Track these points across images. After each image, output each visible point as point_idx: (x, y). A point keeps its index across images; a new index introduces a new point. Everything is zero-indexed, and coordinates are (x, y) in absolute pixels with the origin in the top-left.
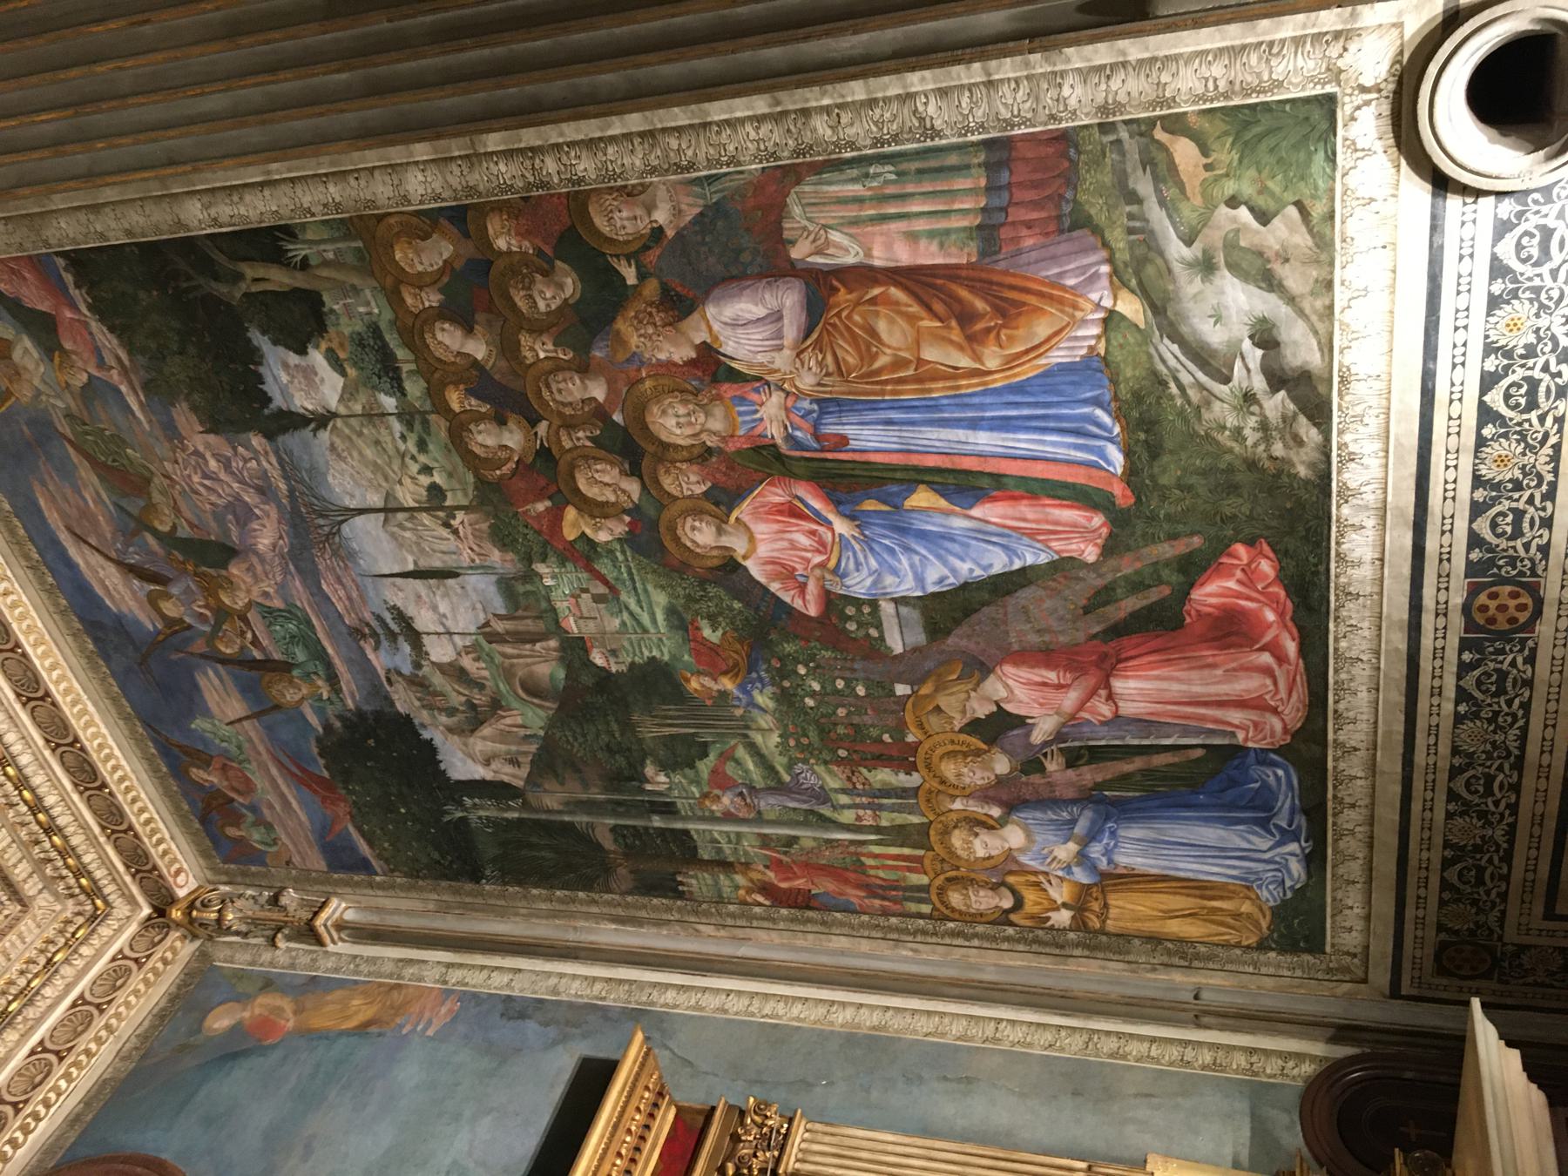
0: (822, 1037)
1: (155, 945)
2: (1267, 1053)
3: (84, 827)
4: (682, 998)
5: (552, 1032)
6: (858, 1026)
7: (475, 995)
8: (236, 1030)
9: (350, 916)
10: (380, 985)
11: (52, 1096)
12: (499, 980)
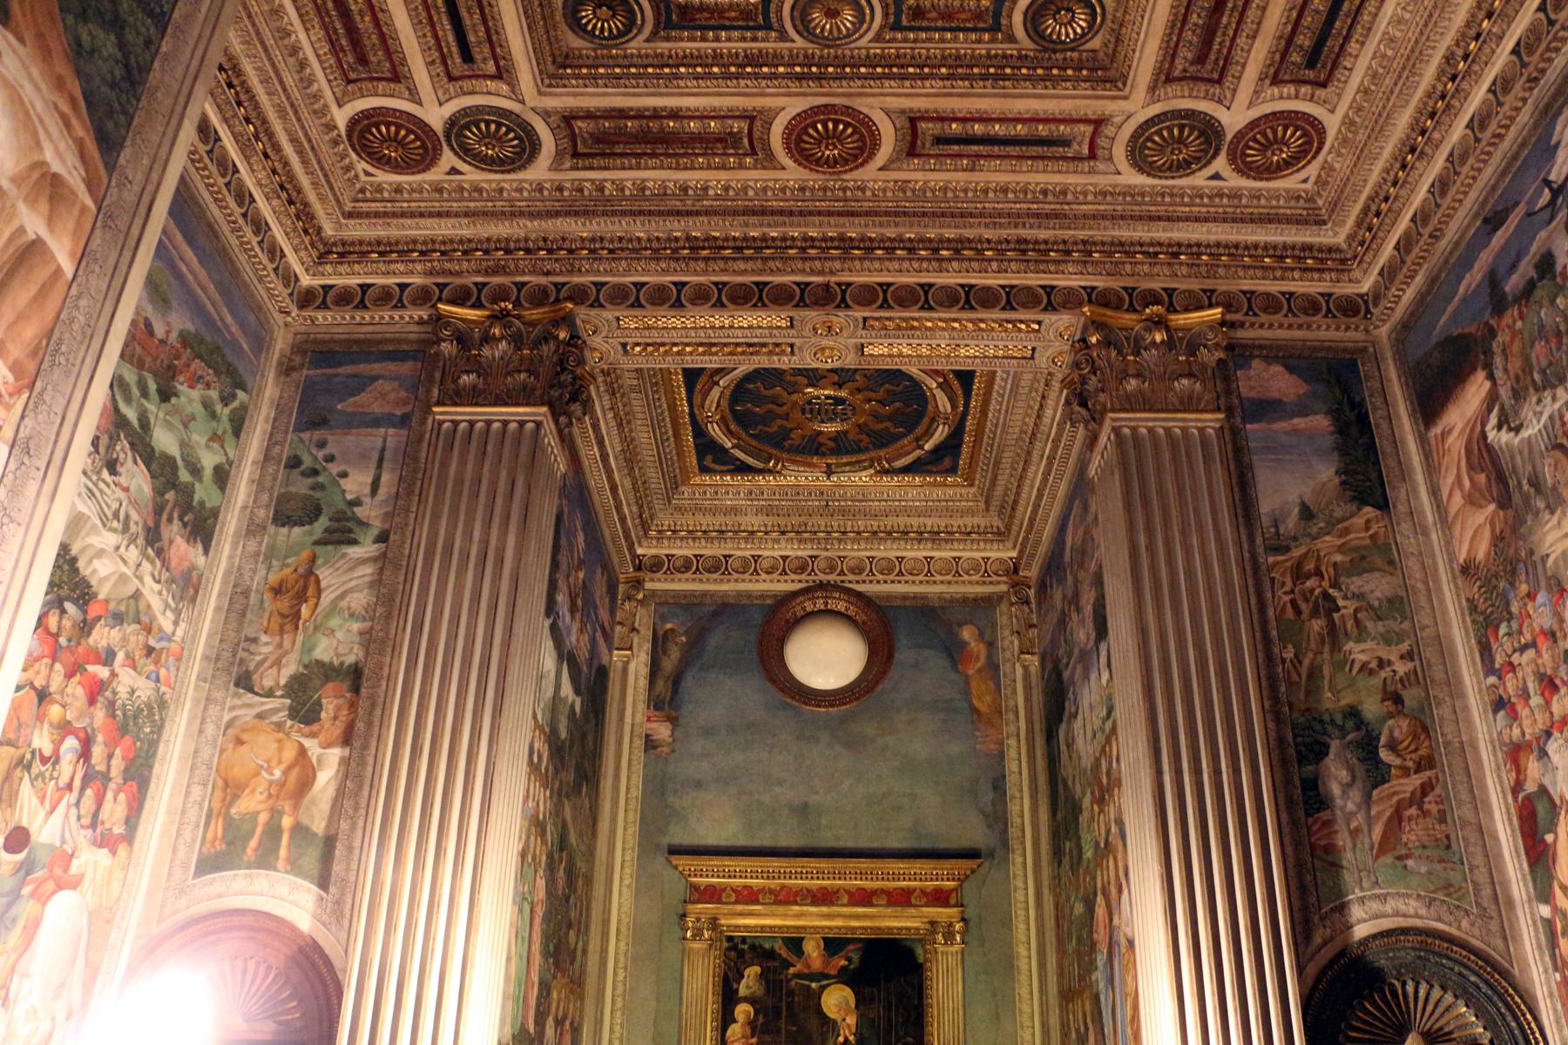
0: (1009, 944)
1: (996, 574)
3: (1022, 524)
4: (1019, 866)
5: (989, 808)
6: (1018, 959)
8: (965, 644)
9: (1033, 670)
12: (1014, 766)
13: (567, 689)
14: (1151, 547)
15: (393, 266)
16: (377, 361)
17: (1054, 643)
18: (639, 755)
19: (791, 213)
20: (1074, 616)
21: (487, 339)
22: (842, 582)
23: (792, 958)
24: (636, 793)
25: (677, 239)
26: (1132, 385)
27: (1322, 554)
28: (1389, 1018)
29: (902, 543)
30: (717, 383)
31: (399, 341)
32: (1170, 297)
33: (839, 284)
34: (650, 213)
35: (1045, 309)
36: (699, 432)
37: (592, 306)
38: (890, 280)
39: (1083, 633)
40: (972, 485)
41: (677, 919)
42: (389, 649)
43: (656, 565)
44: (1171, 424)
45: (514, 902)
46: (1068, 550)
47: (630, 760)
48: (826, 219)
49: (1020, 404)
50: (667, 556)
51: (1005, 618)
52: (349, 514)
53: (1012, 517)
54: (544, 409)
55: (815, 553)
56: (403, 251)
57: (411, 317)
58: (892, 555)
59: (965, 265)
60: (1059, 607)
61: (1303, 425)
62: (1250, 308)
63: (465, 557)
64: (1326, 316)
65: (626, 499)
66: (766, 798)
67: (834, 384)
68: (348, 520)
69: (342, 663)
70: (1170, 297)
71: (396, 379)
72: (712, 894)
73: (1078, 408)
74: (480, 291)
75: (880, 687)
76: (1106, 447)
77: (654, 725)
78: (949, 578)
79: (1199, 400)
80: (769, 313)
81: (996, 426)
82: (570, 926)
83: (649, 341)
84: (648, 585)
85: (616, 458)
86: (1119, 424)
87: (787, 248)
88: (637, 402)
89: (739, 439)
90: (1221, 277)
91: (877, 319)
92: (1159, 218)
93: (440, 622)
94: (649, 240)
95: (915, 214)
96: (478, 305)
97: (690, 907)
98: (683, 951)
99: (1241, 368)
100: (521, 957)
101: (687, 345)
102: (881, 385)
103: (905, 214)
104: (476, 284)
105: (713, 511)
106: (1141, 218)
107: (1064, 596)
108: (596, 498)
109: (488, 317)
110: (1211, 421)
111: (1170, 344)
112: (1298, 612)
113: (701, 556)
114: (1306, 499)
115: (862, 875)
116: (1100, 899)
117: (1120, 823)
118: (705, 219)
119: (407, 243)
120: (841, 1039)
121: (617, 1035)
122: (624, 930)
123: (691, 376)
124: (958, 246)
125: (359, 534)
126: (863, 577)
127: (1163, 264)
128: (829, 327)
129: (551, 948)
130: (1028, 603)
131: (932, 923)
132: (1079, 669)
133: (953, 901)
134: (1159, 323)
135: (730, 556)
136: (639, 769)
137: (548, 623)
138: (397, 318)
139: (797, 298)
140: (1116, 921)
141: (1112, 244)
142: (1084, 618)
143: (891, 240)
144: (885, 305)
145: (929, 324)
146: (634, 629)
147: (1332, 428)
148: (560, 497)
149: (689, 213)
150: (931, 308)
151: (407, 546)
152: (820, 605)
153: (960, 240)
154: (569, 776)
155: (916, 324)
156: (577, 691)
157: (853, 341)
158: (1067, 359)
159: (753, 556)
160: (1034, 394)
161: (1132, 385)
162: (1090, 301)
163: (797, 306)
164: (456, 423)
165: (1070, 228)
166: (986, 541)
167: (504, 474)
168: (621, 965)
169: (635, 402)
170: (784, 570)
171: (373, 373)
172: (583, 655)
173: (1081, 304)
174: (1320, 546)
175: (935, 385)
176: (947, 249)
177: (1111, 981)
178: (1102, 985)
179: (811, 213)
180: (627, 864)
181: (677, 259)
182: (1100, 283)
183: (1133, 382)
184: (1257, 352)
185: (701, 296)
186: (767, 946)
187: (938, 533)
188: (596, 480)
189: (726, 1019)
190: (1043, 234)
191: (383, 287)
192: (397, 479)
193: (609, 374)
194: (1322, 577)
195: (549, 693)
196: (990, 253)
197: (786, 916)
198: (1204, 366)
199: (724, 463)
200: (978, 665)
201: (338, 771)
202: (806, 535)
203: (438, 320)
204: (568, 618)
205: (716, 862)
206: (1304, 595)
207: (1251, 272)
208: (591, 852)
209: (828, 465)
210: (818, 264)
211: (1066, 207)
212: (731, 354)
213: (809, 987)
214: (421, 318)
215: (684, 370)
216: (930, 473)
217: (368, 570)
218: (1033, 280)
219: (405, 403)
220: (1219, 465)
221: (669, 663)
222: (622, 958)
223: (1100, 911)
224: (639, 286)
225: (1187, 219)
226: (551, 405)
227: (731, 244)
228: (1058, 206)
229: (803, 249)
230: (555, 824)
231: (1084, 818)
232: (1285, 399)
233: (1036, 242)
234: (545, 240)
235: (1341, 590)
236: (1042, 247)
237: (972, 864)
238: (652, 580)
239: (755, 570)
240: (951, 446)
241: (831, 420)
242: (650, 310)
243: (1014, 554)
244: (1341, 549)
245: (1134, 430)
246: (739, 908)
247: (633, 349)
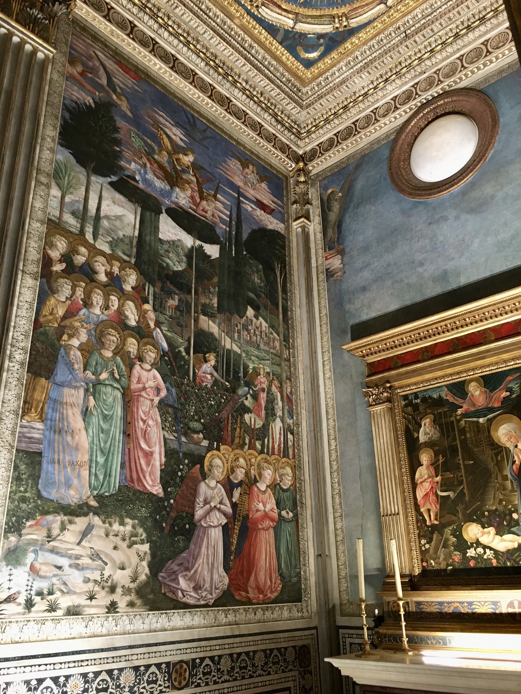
11: (501, 56)
18: (324, 285)
23: (458, 401)
43: (313, 155)
47: (318, 290)
77: (330, 261)
85: (208, 74)
121: (337, 491)
122: (330, 410)
136: (325, 294)
168: (332, 437)
180: (326, 363)
213: (478, 422)
222: (332, 432)
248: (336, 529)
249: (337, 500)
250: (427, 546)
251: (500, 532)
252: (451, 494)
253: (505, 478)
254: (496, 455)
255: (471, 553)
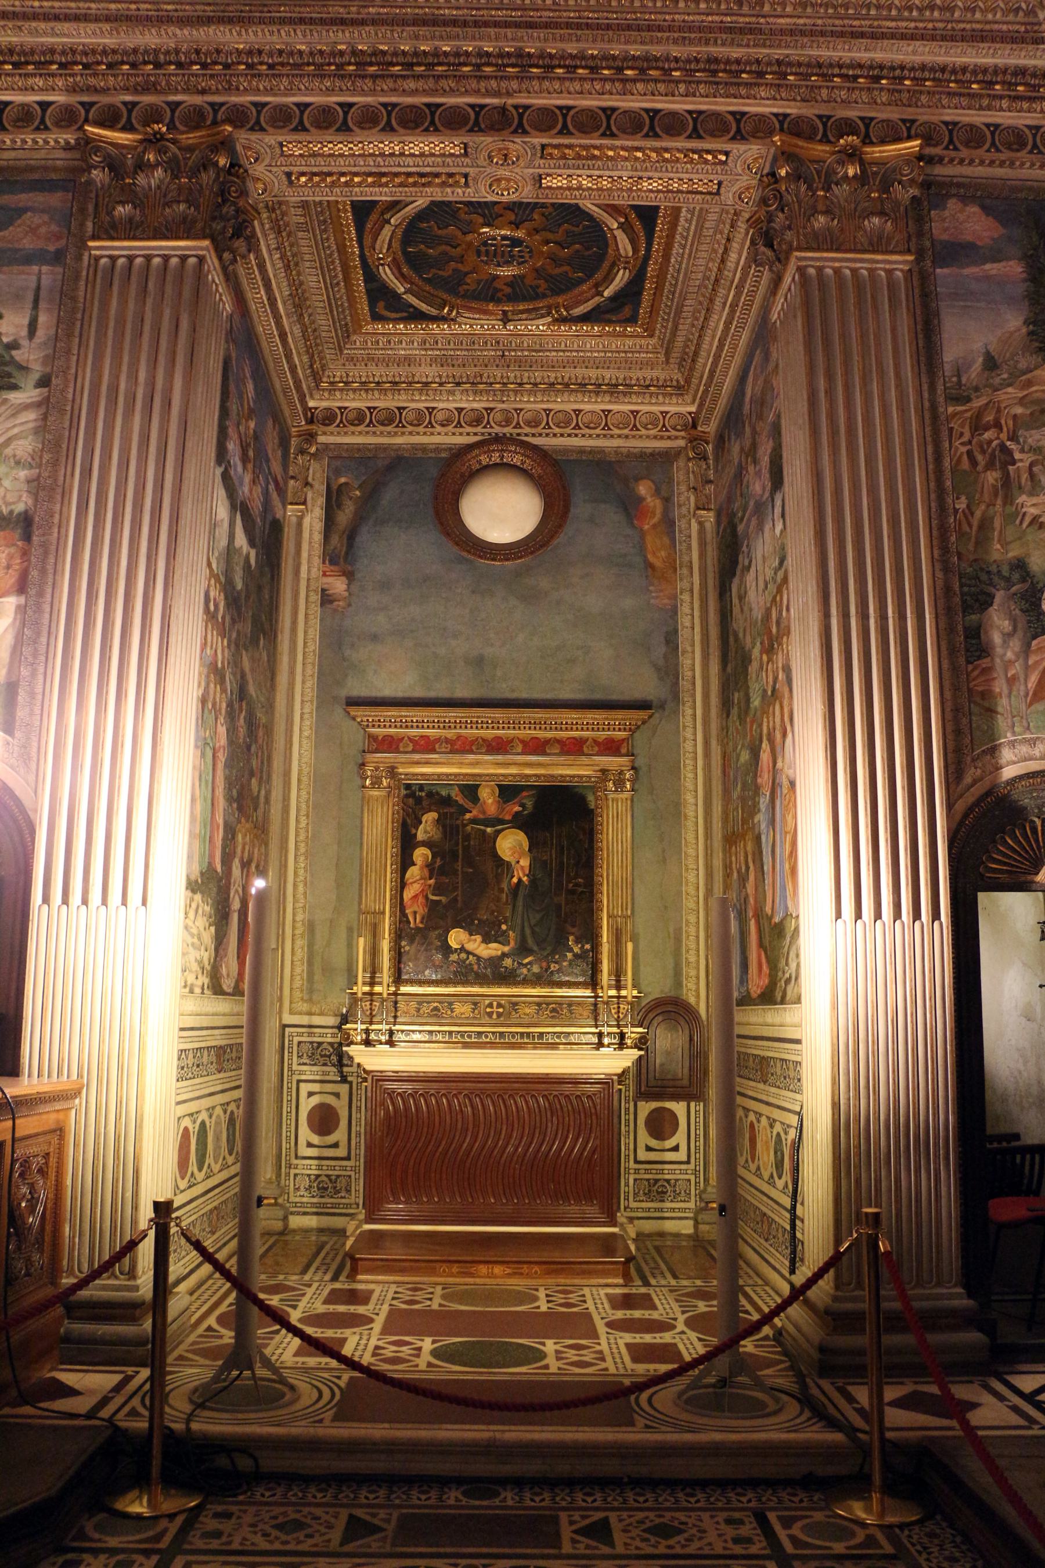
0: (678, 793)
1: (675, 429)
2: (698, 984)
3: (702, 377)
4: (689, 718)
5: (661, 662)
7: (676, 613)
8: (641, 499)
9: (708, 525)
10: (675, 561)
13: (241, 540)
14: (830, 392)
15: (30, 81)
16: (22, 192)
17: (730, 499)
18: (316, 609)
19: (465, 24)
20: (751, 469)
21: (141, 166)
22: (519, 435)
23: (468, 805)
24: (313, 646)
25: (342, 53)
26: (821, 221)
27: (1003, 405)
28: (1027, 852)
29: (580, 395)
30: (388, 222)
31: (46, 168)
32: (867, 126)
33: (516, 107)
34: (312, 21)
35: (733, 138)
36: (371, 276)
37: (252, 129)
38: (570, 103)
39: (758, 485)
40: (651, 336)
41: (356, 769)
42: (59, 497)
43: (329, 418)
44: (859, 265)
45: (196, 747)
46: (747, 399)
47: (306, 614)
48: (502, 31)
49: (704, 247)
50: (340, 408)
51: (682, 473)
52: (7, 358)
53: (692, 369)
54: (206, 243)
55: (491, 405)
56: (40, 63)
57: (56, 141)
58: (569, 407)
59: (651, 86)
60: (736, 461)
61: (994, 272)
62: (951, 141)
63: (131, 399)
64: (1031, 152)
65: (296, 348)
66: (442, 651)
67: (511, 223)
68: (6, 364)
69: (11, 512)
70: (867, 126)
71: (43, 211)
72: (390, 744)
73: (763, 249)
74: (130, 112)
75: (555, 542)
76: (789, 289)
77: (329, 580)
78: (626, 431)
79: (889, 239)
80: (441, 138)
81: (679, 271)
82: (252, 774)
83: (315, 170)
84: (321, 439)
85: (284, 303)
86: (804, 263)
87: (460, 64)
88: (305, 242)
89: (412, 283)
90: (923, 106)
91: (555, 147)
92: (863, 35)
93: (109, 469)
94: (311, 53)
95: (598, 27)
96: (128, 128)
97: (370, 757)
98: (363, 798)
99: (936, 207)
100: (205, 800)
101: (356, 174)
102: (560, 225)
103: (588, 26)
104: (125, 103)
105: (387, 362)
106: (842, 35)
107: (742, 449)
108: (264, 344)
109: (141, 142)
110: (900, 262)
111: (862, 179)
112: (974, 462)
113: (375, 408)
114: (991, 348)
115: (536, 724)
116: (765, 745)
117: (787, 670)
118: (371, 29)
119: (44, 53)
120: (515, 880)
122: (305, 779)
123: (362, 210)
124: (644, 64)
125: (18, 378)
126: (539, 430)
127: (861, 89)
128: (506, 155)
129: (235, 793)
130: (705, 458)
131: (604, 771)
132: (754, 522)
133: (624, 751)
134: (852, 155)
135: (404, 408)
137: (219, 471)
138: (41, 142)
139: (471, 123)
140: (779, 765)
141: (809, 65)
142: (760, 470)
143: (573, 57)
144: (564, 131)
145: (611, 153)
146: (307, 484)
147: (1024, 275)
148: (227, 342)
149: (354, 22)
150: (613, 135)
151: (71, 390)
152: (496, 458)
153: (646, 58)
154: (247, 628)
155: (596, 152)
156: (252, 543)
157: (531, 171)
158: (755, 195)
159: (427, 408)
160: (719, 236)
161: (821, 221)
162: (782, 130)
163: (471, 130)
164: (113, 259)
165: (764, 46)
166: (664, 395)
167: (167, 312)
168: (303, 812)
169: (302, 242)
170: (459, 422)
171: (21, 205)
172: (256, 506)
173: (771, 133)
174: (1003, 397)
175: (615, 225)
176: (632, 68)
177: (772, 822)
178: (763, 826)
179: (486, 24)
180: (306, 716)
181: (343, 77)
182: (792, 110)
183: (822, 219)
184: (954, 191)
185: (369, 119)
186: (444, 793)
187: (617, 385)
188: (264, 326)
189: (405, 862)
190: (736, 53)
191: (23, 106)
192: (55, 321)
193: (274, 210)
194: (1001, 429)
195: (224, 542)
196: (677, 74)
197: (461, 764)
198: (897, 203)
199: (396, 311)
200: (655, 520)
201: (15, 619)
202: (481, 386)
203: (86, 144)
204: (240, 469)
205: (392, 713)
206: (981, 447)
207: (955, 100)
208: (270, 707)
209: (505, 312)
210: (493, 83)
211: (762, 20)
212: (401, 185)
214: (67, 143)
215: (352, 202)
216: (609, 322)
217: (31, 416)
218: (724, 105)
219: (59, 238)
220: (905, 311)
221: (344, 517)
222: (304, 806)
223: (765, 756)
224: (303, 107)
225: (893, 36)
226: (214, 240)
227: (401, 59)
228: (753, 19)
229: (478, 67)
230: (234, 674)
231: (753, 668)
232: (979, 243)
233: (728, 62)
234: (197, 52)
235: (1018, 443)
236: (734, 67)
237: (643, 714)
238: (325, 433)
239: (430, 422)
240: (631, 293)
241: (508, 263)
242: (315, 135)
243: (693, 409)
244: (1021, 401)
245: (820, 270)
246: (417, 757)
247: (298, 179)
248: (294, 921)
249: (301, 888)
250: (407, 948)
251: (487, 940)
252: (443, 899)
253: (501, 890)
254: (498, 867)
255: (454, 957)
